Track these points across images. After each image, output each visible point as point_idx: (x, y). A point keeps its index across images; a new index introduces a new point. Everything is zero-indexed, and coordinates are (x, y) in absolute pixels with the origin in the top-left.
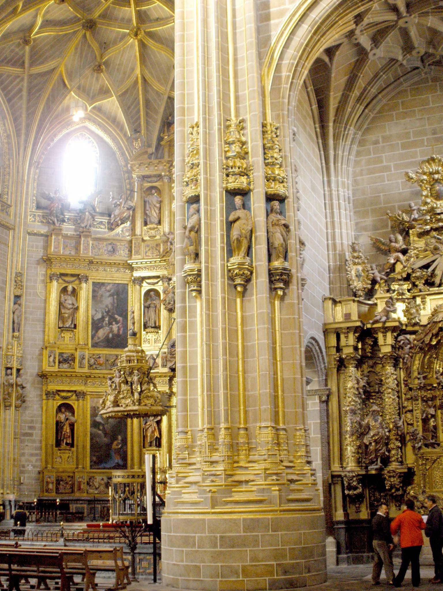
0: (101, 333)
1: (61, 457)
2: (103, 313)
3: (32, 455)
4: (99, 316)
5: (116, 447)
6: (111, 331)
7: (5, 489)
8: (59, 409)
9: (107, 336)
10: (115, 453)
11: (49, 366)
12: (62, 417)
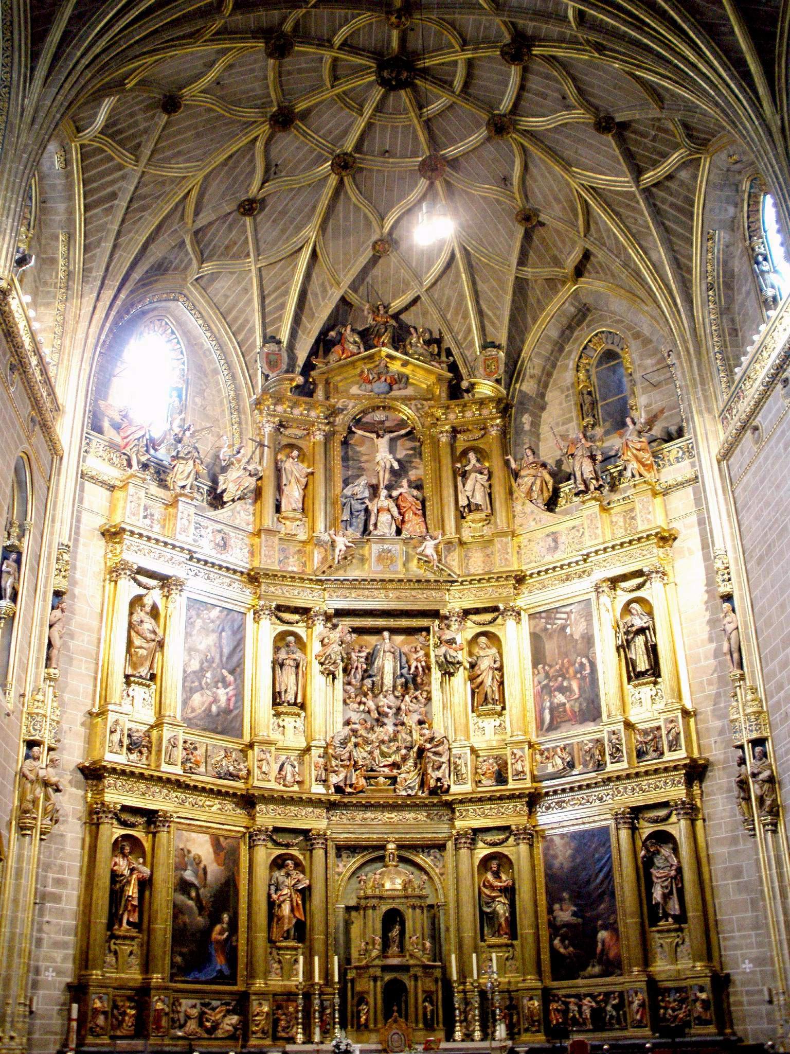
0: (198, 700)
1: (116, 953)
3: (56, 945)
4: (195, 666)
5: (219, 937)
6: (216, 700)
8: (118, 847)
9: (209, 709)
11: (111, 752)
12: (122, 865)
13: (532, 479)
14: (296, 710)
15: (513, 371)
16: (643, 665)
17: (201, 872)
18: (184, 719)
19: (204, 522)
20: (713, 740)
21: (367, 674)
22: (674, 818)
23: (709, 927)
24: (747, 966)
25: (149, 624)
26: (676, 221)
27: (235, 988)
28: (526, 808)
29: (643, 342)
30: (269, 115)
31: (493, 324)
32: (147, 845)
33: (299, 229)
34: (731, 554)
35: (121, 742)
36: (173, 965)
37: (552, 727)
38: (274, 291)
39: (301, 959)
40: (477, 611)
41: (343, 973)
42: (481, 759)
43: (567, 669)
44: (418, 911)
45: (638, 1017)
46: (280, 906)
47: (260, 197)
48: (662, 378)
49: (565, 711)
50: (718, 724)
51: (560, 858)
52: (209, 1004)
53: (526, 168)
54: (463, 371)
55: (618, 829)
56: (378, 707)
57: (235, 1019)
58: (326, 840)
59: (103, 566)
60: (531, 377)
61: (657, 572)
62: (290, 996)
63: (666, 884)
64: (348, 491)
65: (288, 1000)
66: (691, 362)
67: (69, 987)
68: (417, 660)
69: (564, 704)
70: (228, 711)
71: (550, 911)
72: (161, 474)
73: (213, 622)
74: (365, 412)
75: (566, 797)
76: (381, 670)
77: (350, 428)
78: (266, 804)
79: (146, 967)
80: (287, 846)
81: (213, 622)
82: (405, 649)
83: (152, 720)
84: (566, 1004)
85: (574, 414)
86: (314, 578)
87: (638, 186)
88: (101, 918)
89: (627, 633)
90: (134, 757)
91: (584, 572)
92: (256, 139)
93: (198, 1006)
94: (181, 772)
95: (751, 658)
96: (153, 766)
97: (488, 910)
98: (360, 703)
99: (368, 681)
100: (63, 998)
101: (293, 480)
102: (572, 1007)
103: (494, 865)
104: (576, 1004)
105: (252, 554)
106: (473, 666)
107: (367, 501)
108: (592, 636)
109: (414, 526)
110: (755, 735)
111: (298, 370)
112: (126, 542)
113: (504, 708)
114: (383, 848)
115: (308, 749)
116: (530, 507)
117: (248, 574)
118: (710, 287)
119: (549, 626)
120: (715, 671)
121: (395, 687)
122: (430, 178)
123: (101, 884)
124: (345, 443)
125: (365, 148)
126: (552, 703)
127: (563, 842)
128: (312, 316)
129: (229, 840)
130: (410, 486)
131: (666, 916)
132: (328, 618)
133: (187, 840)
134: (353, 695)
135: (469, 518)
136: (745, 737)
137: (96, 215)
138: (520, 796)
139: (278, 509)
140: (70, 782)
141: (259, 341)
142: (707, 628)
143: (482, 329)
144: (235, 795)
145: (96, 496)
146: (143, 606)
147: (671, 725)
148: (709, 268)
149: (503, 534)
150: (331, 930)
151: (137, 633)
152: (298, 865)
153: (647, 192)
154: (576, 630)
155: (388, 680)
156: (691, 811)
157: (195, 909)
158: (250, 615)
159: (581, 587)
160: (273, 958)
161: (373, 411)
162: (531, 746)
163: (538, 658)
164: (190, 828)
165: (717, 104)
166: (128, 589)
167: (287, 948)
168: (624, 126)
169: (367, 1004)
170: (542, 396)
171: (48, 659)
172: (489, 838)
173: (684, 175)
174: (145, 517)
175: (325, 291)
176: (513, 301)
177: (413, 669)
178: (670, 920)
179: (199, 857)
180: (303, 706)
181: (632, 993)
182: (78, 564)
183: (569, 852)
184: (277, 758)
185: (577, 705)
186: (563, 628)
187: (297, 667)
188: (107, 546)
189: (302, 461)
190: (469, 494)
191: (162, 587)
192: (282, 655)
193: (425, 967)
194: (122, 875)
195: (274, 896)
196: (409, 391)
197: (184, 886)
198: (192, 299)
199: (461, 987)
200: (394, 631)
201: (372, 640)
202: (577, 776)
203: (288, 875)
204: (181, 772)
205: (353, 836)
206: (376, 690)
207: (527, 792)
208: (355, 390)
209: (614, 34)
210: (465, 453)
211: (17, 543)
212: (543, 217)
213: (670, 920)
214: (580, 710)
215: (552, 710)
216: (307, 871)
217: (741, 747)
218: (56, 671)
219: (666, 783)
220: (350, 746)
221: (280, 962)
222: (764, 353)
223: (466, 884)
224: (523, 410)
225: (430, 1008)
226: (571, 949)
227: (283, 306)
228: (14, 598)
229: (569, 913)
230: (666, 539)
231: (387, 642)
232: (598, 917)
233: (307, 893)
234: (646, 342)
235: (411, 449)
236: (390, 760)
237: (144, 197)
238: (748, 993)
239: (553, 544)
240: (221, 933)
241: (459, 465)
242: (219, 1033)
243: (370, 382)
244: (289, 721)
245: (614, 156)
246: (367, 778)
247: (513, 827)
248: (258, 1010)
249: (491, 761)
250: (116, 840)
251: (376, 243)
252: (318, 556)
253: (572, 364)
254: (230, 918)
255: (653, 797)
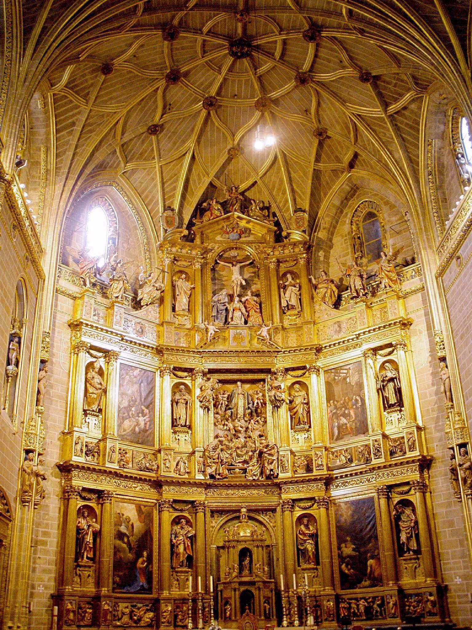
0: (127, 423)
1: (80, 576)
2: (129, 402)
3: (44, 571)
4: (125, 404)
5: (141, 566)
7: (16, 619)
8: (80, 512)
9: (134, 430)
10: (140, 574)
12: (83, 523)
13: (325, 290)
14: (186, 429)
15: (313, 225)
16: (393, 400)
17: (130, 527)
18: (119, 435)
19: (130, 318)
20: (435, 444)
21: (228, 408)
22: (412, 492)
23: (435, 558)
24: (458, 580)
25: (97, 379)
26: (409, 134)
27: (151, 596)
28: (324, 487)
29: (390, 206)
30: (165, 74)
31: (300, 197)
32: (98, 512)
33: (184, 142)
34: (444, 332)
35: (81, 449)
36: (114, 583)
37: (339, 438)
38: (170, 179)
39: (191, 578)
40: (293, 369)
41: (215, 587)
42: (296, 458)
43: (348, 403)
44: (260, 549)
45: (393, 611)
46: (177, 547)
47: (160, 123)
48: (402, 228)
49: (347, 427)
50: (438, 434)
51: (345, 516)
52: (136, 606)
53: (319, 104)
54: (283, 226)
55: (379, 498)
56: (234, 427)
57: (151, 614)
58: (205, 507)
59: (69, 345)
60: (324, 229)
61: (401, 345)
62: (184, 600)
63: (408, 531)
64: (215, 298)
65: (183, 603)
66: (419, 219)
67: (52, 596)
68: (257, 399)
69: (346, 424)
70: (145, 431)
71: (339, 548)
72: (104, 290)
73: (135, 377)
74: (224, 251)
75: (348, 479)
76: (236, 405)
77: (216, 261)
78: (169, 486)
79: (98, 584)
80: (182, 511)
81: (135, 377)
82: (251, 392)
83: (100, 436)
84: (350, 604)
85: (350, 250)
86: (196, 350)
87: (386, 113)
88: (71, 555)
89: (383, 381)
90: (89, 458)
91: (357, 345)
92: (158, 89)
93: (130, 607)
94: (118, 468)
95: (458, 395)
96: (101, 464)
97: (302, 548)
98: (224, 425)
99: (229, 412)
100: (49, 603)
101: (182, 292)
102: (353, 606)
103: (305, 520)
104: (356, 604)
105: (159, 337)
106: (291, 402)
107: (227, 304)
108: (363, 383)
109: (255, 318)
110: (460, 441)
111: (185, 226)
112: (83, 330)
113: (310, 427)
114: (239, 511)
115: (194, 453)
116: (324, 306)
117: (157, 349)
118: (430, 174)
119: (336, 378)
120: (436, 403)
121: (244, 415)
122: (261, 111)
123: (71, 534)
124: (213, 270)
125: (223, 94)
126: (339, 424)
127: (346, 506)
128: (193, 194)
129: (146, 508)
130: (252, 295)
131: (409, 550)
132: (204, 374)
133: (122, 508)
134: (220, 420)
135: (288, 313)
136: (455, 442)
137: (63, 135)
138: (320, 480)
139: (174, 309)
140: (52, 474)
141: (161, 209)
142: (431, 377)
143: (295, 200)
144: (150, 480)
145: (65, 303)
146: (94, 368)
147: (410, 436)
148: (429, 162)
149: (308, 323)
150: (209, 561)
151: (91, 384)
152: (188, 522)
153: (391, 117)
154: (353, 380)
155: (241, 411)
156: (423, 488)
157: (127, 549)
158: (158, 373)
159: (356, 353)
160: (174, 578)
161: (230, 250)
162: (326, 449)
163: (330, 396)
164: (123, 501)
165: (432, 64)
166: (85, 358)
167: (182, 572)
168: (377, 78)
169: (230, 605)
170: (331, 240)
171: (38, 400)
172: (302, 504)
173: (413, 106)
174: (94, 315)
175: (200, 179)
176: (312, 183)
177: (255, 404)
178: (411, 552)
179: (129, 518)
180: (190, 427)
181: (388, 597)
182: (55, 344)
183: (350, 512)
184: (174, 458)
185: (354, 424)
186: (345, 379)
187: (186, 403)
188: (72, 333)
189: (188, 281)
190: (288, 299)
191: (105, 357)
192: (177, 397)
193: (264, 582)
194: (83, 529)
195: (174, 541)
196: (251, 238)
197: (120, 536)
198: (120, 185)
199: (287, 594)
200: (243, 382)
201: (231, 387)
202: (354, 467)
203: (182, 528)
204: (118, 468)
205: (221, 504)
206: (233, 417)
207: (324, 477)
208: (219, 238)
209: (370, 23)
210: (285, 275)
211: (18, 331)
212: (329, 133)
213: (411, 552)
214: (356, 428)
215: (339, 428)
216: (194, 525)
217: (452, 448)
218: (42, 408)
219: (407, 471)
220: (218, 450)
221: (178, 580)
222: (463, 212)
223: (288, 531)
224: (319, 248)
225: (268, 607)
226: (352, 571)
227: (175, 189)
228: (17, 365)
229: (351, 549)
230: (405, 324)
231: (240, 388)
232: (367, 551)
233: (194, 539)
234: (392, 207)
235: (253, 273)
236: (243, 459)
237: (91, 125)
238: (459, 596)
239: (338, 329)
240: (142, 563)
241: (281, 282)
242: (142, 623)
243: (228, 233)
244: (182, 437)
245: (371, 96)
246: (229, 470)
247: (317, 498)
248: (165, 609)
249: (303, 458)
250: (79, 508)
251: (230, 150)
252: (197, 338)
253: (348, 221)
254: (148, 555)
255: (400, 479)
